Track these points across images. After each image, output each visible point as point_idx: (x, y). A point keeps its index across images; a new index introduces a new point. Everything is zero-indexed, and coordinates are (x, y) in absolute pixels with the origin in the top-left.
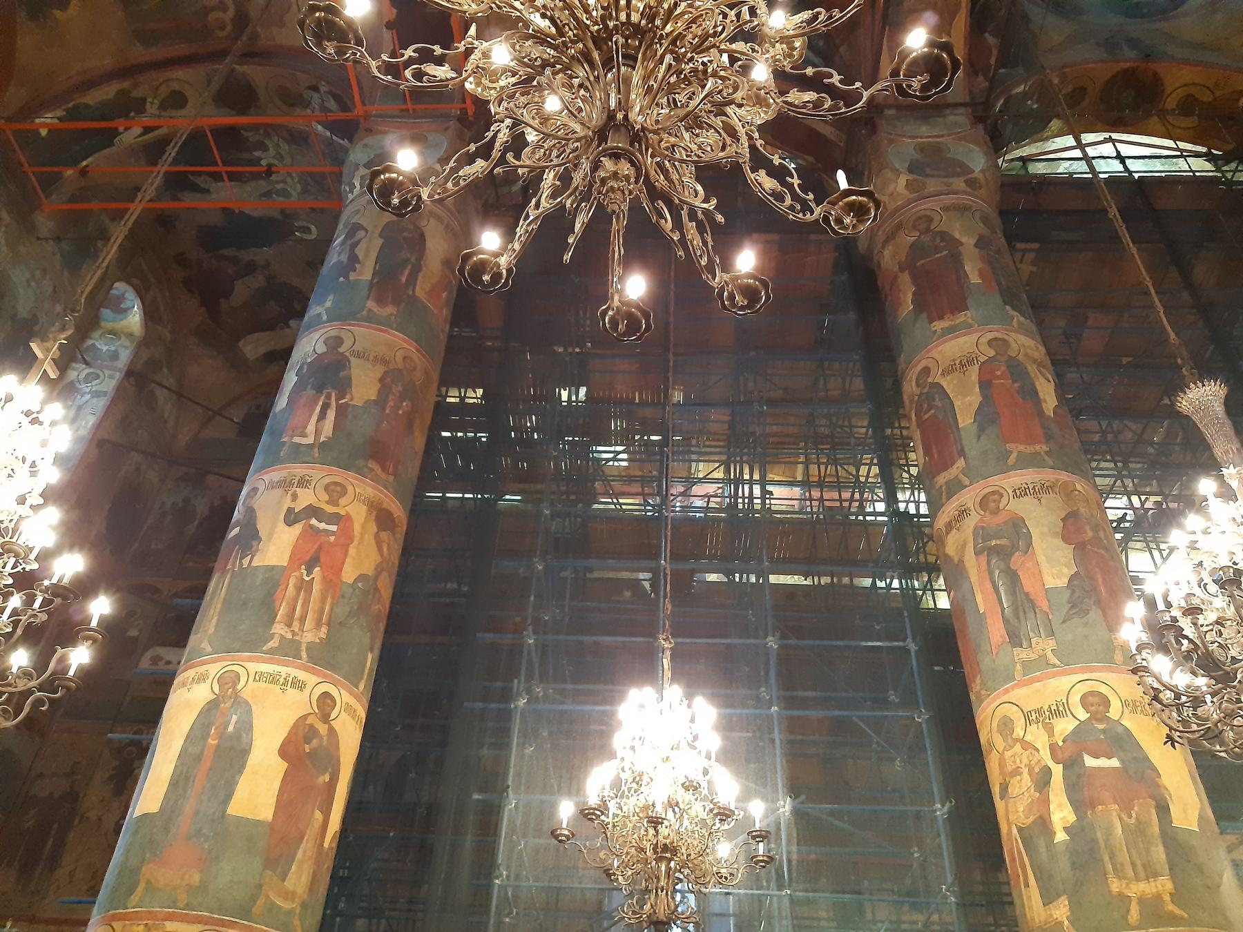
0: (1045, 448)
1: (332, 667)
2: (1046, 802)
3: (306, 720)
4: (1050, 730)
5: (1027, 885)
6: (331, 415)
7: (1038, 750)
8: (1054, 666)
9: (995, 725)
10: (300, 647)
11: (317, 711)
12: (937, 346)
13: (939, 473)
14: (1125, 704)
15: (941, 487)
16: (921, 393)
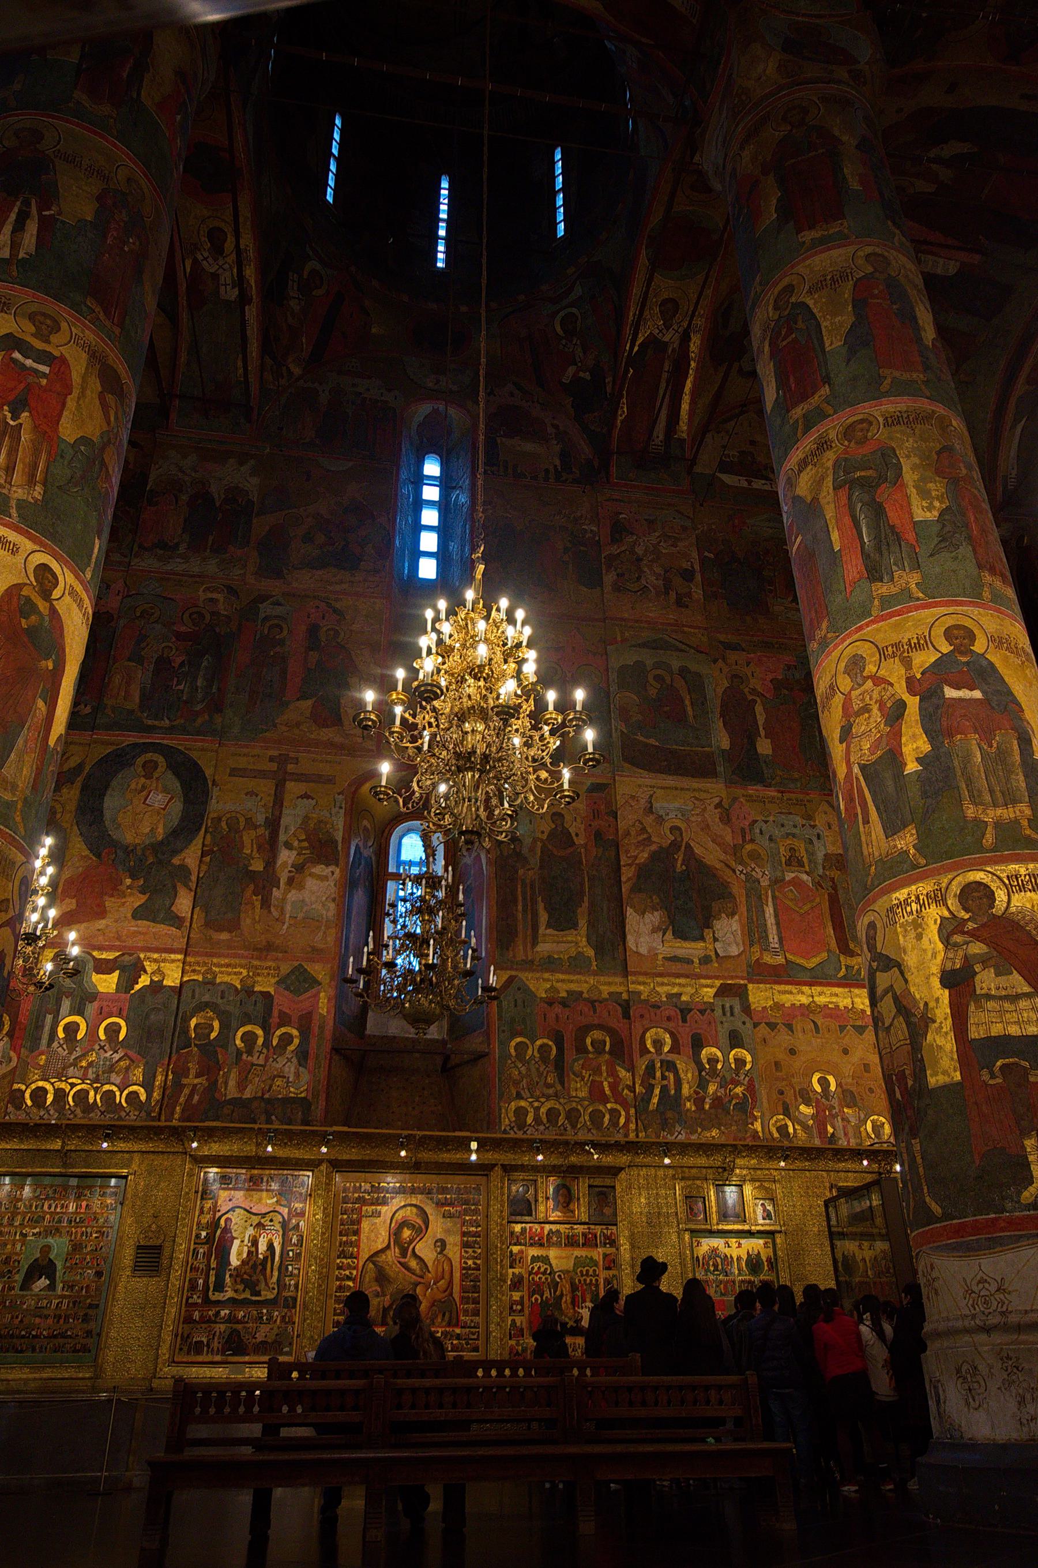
0: (921, 376)
1: (53, 536)
2: (899, 735)
3: (21, 589)
4: (907, 663)
5: (866, 822)
6: (32, 227)
7: (892, 685)
8: (918, 599)
9: (842, 665)
10: (9, 502)
11: (35, 584)
12: (804, 260)
13: (796, 404)
14: (991, 639)
15: (797, 421)
16: (780, 317)
